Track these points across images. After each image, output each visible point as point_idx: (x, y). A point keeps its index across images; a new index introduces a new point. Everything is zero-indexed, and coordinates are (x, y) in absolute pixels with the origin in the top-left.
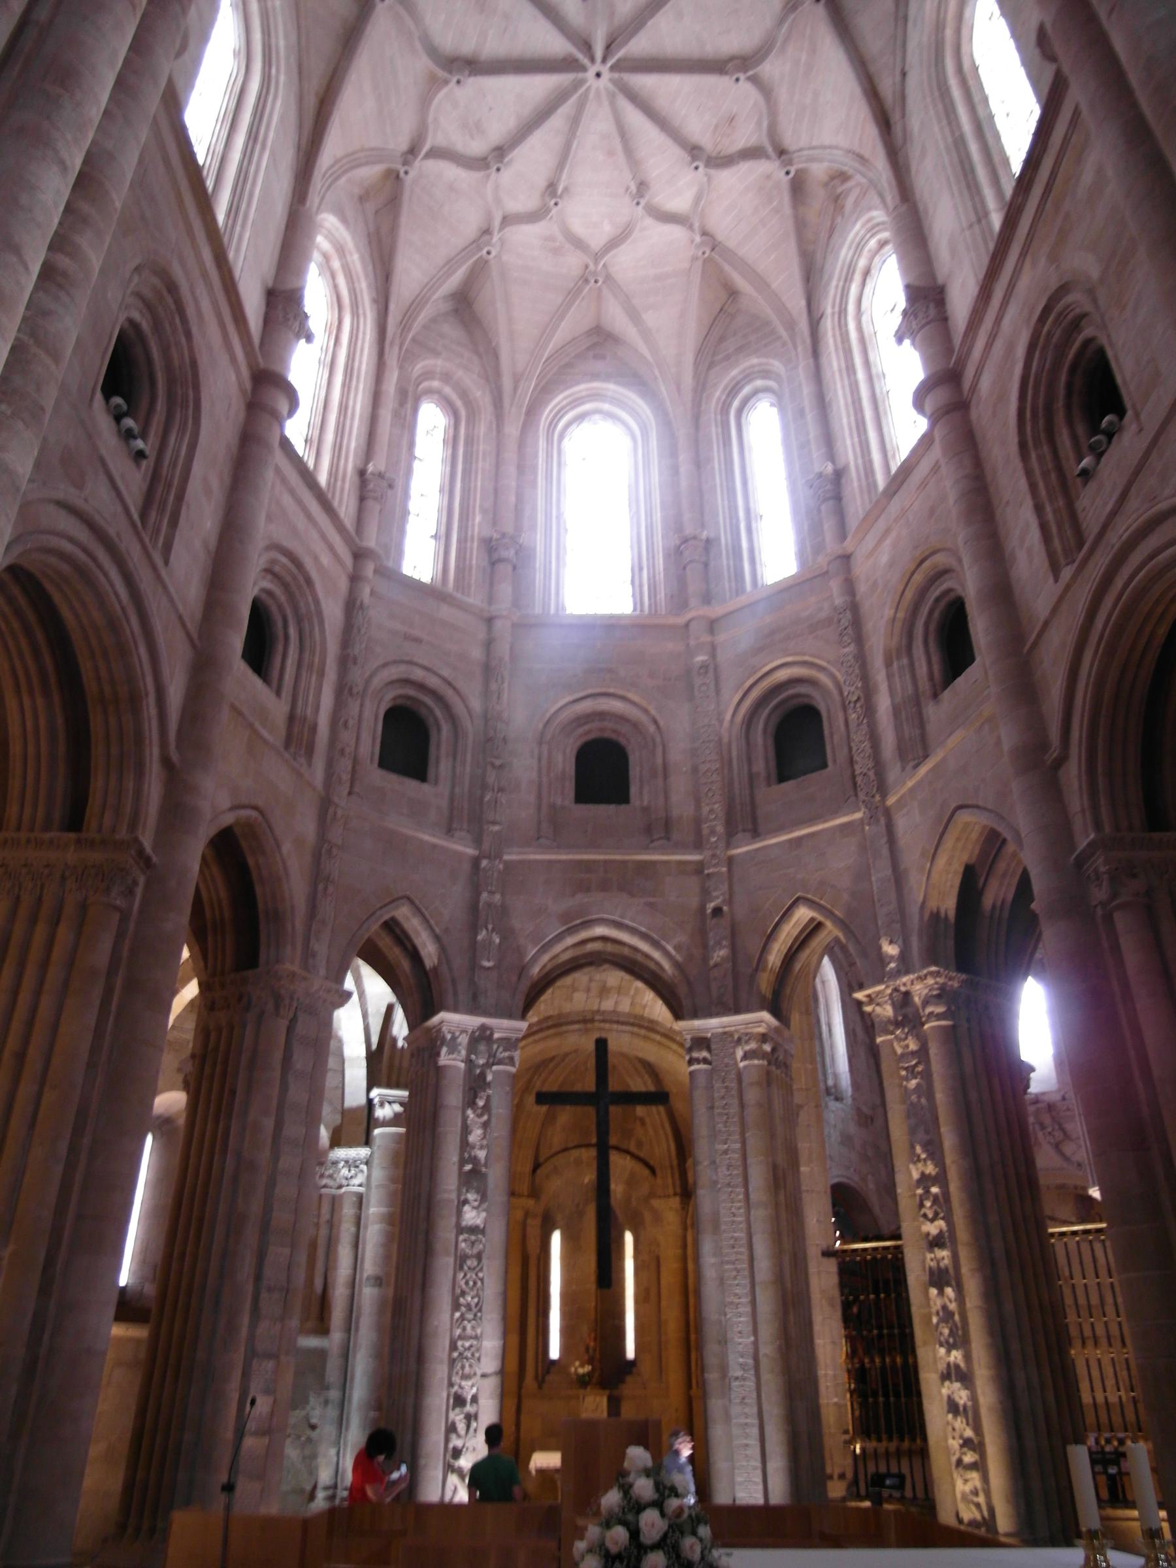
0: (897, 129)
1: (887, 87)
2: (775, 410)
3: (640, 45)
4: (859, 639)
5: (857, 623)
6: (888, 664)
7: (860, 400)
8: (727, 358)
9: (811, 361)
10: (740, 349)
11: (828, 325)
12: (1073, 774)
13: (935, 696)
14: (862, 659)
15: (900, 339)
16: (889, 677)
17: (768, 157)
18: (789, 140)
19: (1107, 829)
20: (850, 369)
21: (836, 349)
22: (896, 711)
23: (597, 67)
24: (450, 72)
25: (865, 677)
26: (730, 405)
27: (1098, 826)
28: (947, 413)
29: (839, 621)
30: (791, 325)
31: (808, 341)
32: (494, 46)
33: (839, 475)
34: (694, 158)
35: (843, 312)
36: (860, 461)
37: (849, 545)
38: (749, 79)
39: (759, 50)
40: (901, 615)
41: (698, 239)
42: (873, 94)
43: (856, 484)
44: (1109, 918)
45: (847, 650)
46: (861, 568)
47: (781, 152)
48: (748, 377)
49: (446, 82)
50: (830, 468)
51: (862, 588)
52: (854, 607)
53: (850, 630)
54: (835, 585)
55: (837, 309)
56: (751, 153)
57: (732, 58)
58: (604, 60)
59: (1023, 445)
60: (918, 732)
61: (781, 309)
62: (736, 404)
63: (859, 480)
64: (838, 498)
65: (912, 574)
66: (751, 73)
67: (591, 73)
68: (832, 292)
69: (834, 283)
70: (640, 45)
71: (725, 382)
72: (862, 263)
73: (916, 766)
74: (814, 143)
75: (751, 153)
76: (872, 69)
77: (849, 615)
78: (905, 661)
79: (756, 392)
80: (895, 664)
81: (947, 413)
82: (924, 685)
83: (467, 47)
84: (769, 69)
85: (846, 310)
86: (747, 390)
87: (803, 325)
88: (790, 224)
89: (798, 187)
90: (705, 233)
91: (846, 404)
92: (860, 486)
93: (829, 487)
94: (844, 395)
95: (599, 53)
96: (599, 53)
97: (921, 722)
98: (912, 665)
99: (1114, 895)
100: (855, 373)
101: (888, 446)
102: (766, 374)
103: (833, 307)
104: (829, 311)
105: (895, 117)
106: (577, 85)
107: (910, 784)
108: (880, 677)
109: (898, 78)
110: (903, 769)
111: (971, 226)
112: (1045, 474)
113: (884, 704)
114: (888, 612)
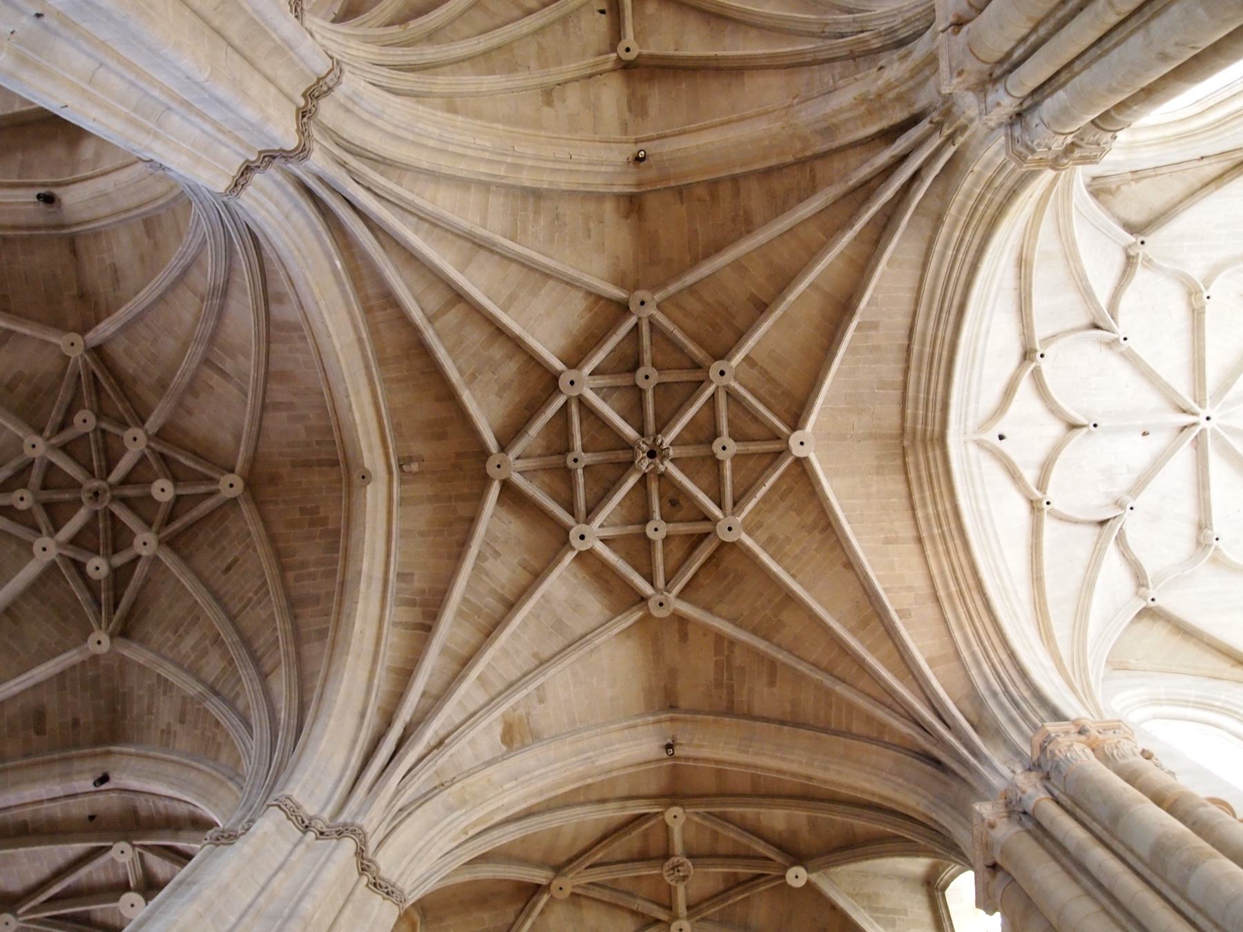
3: (1182, 386)
23: (1202, 419)
24: (1210, 546)
32: (1186, 508)
38: (1207, 288)
49: (1216, 549)
66: (1203, 288)
70: (1182, 386)
83: (1188, 531)
84: (1196, 272)
95: (1191, 419)
96: (1191, 419)
106: (1216, 435)
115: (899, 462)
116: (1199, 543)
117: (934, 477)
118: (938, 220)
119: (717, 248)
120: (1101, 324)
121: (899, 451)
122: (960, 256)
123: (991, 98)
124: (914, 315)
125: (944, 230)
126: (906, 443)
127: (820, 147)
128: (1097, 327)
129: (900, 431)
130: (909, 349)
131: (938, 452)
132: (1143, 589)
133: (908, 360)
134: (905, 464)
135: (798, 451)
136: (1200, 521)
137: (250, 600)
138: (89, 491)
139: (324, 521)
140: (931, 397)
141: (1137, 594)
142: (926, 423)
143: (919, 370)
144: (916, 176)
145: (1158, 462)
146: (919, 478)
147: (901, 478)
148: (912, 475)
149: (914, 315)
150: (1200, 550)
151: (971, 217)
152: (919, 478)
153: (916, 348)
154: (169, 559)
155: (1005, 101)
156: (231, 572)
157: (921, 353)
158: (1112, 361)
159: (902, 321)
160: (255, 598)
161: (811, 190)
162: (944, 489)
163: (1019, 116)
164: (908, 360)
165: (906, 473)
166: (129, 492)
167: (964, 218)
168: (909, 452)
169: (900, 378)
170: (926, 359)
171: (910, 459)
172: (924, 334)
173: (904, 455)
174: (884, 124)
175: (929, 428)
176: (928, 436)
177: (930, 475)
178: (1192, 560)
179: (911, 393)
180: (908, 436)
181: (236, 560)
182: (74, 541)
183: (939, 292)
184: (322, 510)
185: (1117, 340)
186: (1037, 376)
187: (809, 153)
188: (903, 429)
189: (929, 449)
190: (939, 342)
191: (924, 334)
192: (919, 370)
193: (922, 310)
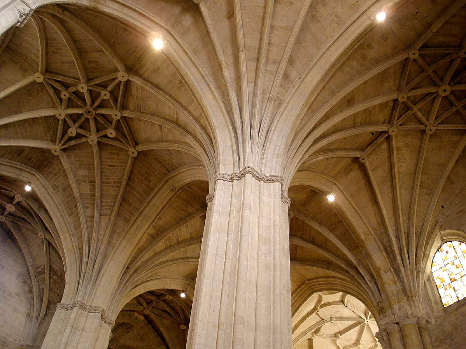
23: (367, 320)
58: (367, 319)
67: (365, 322)
83: (337, 330)
96: (365, 319)
115: (300, 284)
116: (335, 334)
126: (306, 282)
131: (309, 292)
132: (314, 334)
136: (341, 331)
137: (110, 182)
138: (88, 109)
139: (150, 181)
141: (312, 333)
145: (348, 318)
146: (300, 292)
148: (299, 290)
150: (334, 336)
152: (300, 292)
154: (95, 149)
156: (111, 168)
160: (112, 184)
162: (301, 301)
166: (97, 103)
171: (303, 286)
173: (303, 284)
175: (314, 287)
176: (312, 287)
177: (302, 294)
178: (330, 336)
181: (115, 166)
182: (70, 115)
184: (152, 177)
188: (309, 280)
189: (309, 289)
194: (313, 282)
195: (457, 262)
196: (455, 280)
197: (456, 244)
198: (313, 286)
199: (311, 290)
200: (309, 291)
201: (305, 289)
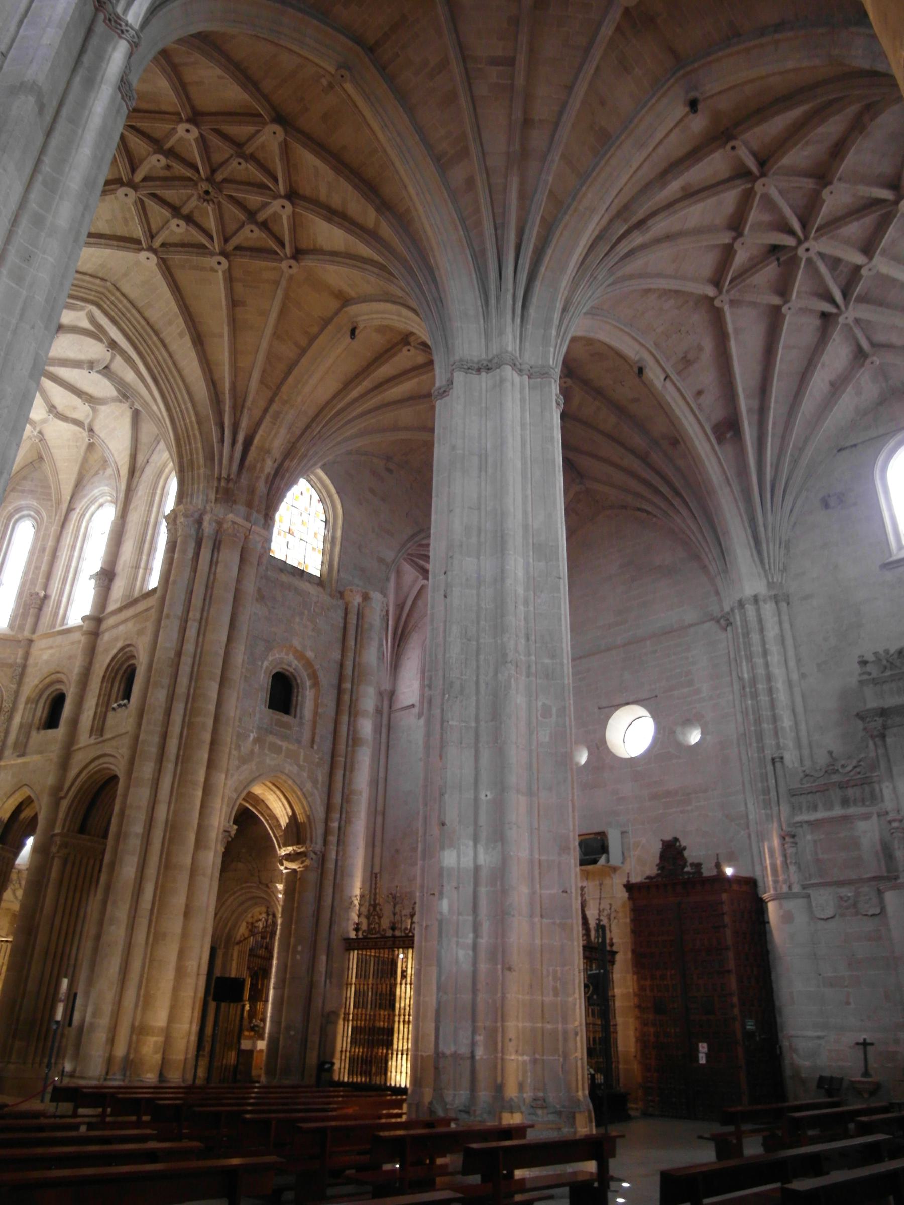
0: (135, 480)
1: (140, 459)
2: (32, 531)
4: (20, 683)
5: (22, 675)
6: (26, 704)
7: (70, 566)
8: (23, 491)
9: (59, 529)
10: (31, 491)
11: (74, 516)
12: (65, 804)
13: (38, 729)
14: (17, 693)
15: (90, 579)
16: (25, 709)
17: (84, 429)
18: (96, 428)
19: (65, 831)
20: (73, 547)
21: (72, 532)
22: (21, 726)
25: (15, 703)
26: (14, 515)
27: (63, 828)
28: (90, 634)
29: (15, 670)
30: (59, 502)
31: (63, 518)
33: (46, 597)
34: (50, 411)
35: (83, 515)
36: (57, 598)
37: (34, 637)
39: (100, 399)
40: (40, 686)
41: (35, 433)
42: (133, 457)
43: (50, 609)
44: (53, 858)
45: (12, 686)
46: (35, 651)
47: (91, 430)
48: (28, 507)
50: (42, 594)
51: (31, 661)
52: (24, 667)
53: (17, 678)
54: (20, 652)
55: (81, 512)
56: (77, 423)
57: (87, 394)
59: (104, 677)
60: (25, 740)
61: (59, 491)
62: (17, 516)
63: (52, 608)
64: (40, 609)
65: (53, 674)
68: (83, 503)
69: (86, 500)
71: (15, 504)
72: (101, 500)
73: (19, 756)
74: (106, 441)
75: (77, 423)
76: (138, 446)
77: (20, 670)
78: (34, 706)
79: (29, 515)
80: (29, 706)
81: (90, 634)
82: (36, 721)
85: (85, 515)
86: (25, 512)
87: (65, 506)
88: (80, 460)
89: (91, 447)
90: (40, 432)
91: (64, 564)
92: (51, 611)
93: (39, 602)
94: (65, 560)
97: (28, 736)
98: (35, 710)
99: (58, 852)
100: (74, 551)
101: (71, 598)
102: (38, 512)
103: (81, 510)
104: (78, 510)
105: (137, 475)
107: (12, 762)
108: (21, 706)
109: (145, 461)
110: (12, 753)
111: (132, 567)
112: (105, 695)
113: (17, 720)
114: (36, 682)
115: (100, 275)
117: (79, 289)
118: (199, 423)
119: (282, 313)
120: (105, 370)
121: (106, 278)
122: (178, 409)
123: (214, 524)
124: (171, 356)
125: (194, 419)
126: (109, 284)
127: (275, 407)
128: (106, 367)
129: (117, 286)
130: (157, 334)
131: (92, 298)
133: (151, 327)
134: (97, 277)
135: (144, 254)
140: (124, 319)
142: (112, 303)
143: (142, 327)
144: (222, 441)
147: (90, 271)
148: (88, 278)
149: (171, 356)
151: (188, 437)
152: (84, 281)
153: (155, 338)
155: (208, 528)
157: (151, 339)
158: (82, 357)
159: (173, 347)
161: (262, 381)
163: (199, 522)
164: (151, 327)
165: (91, 275)
167: (191, 433)
168: (102, 283)
169: (146, 314)
170: (146, 337)
171: (98, 281)
172: (158, 349)
173: (103, 279)
174: (253, 449)
175: (108, 303)
179: (134, 311)
180: (112, 288)
183: (172, 380)
185: (92, 369)
186: (101, 341)
187: (277, 399)
188: (118, 289)
190: (150, 353)
191: (158, 349)
192: (142, 327)
193: (170, 363)
194: (117, 298)
195: (305, 516)
196: (293, 534)
197: (316, 497)
198: (108, 299)
199: (98, 297)
200: (94, 296)
201: (95, 287)
